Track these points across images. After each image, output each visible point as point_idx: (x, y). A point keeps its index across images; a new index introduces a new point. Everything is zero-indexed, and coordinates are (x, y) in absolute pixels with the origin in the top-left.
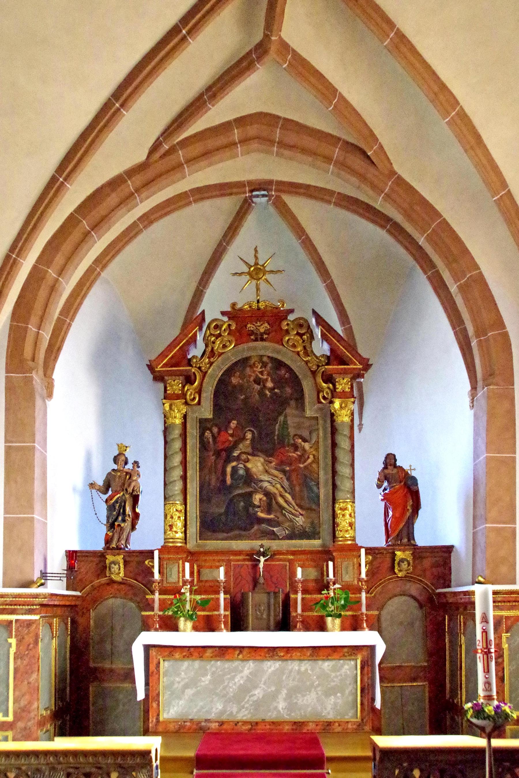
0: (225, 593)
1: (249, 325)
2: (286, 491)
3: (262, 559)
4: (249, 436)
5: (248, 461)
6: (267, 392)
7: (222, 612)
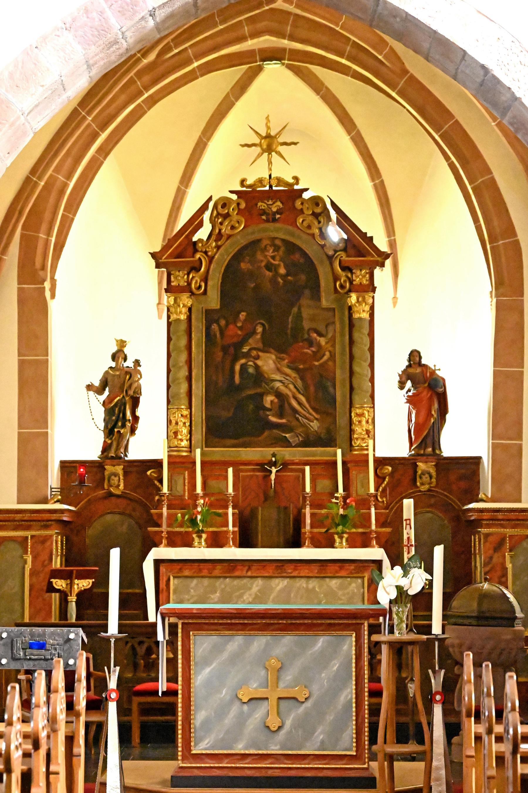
0: (234, 508)
1: (260, 204)
2: (300, 393)
3: (274, 470)
4: (260, 329)
5: (258, 357)
6: (280, 280)
7: (231, 528)
